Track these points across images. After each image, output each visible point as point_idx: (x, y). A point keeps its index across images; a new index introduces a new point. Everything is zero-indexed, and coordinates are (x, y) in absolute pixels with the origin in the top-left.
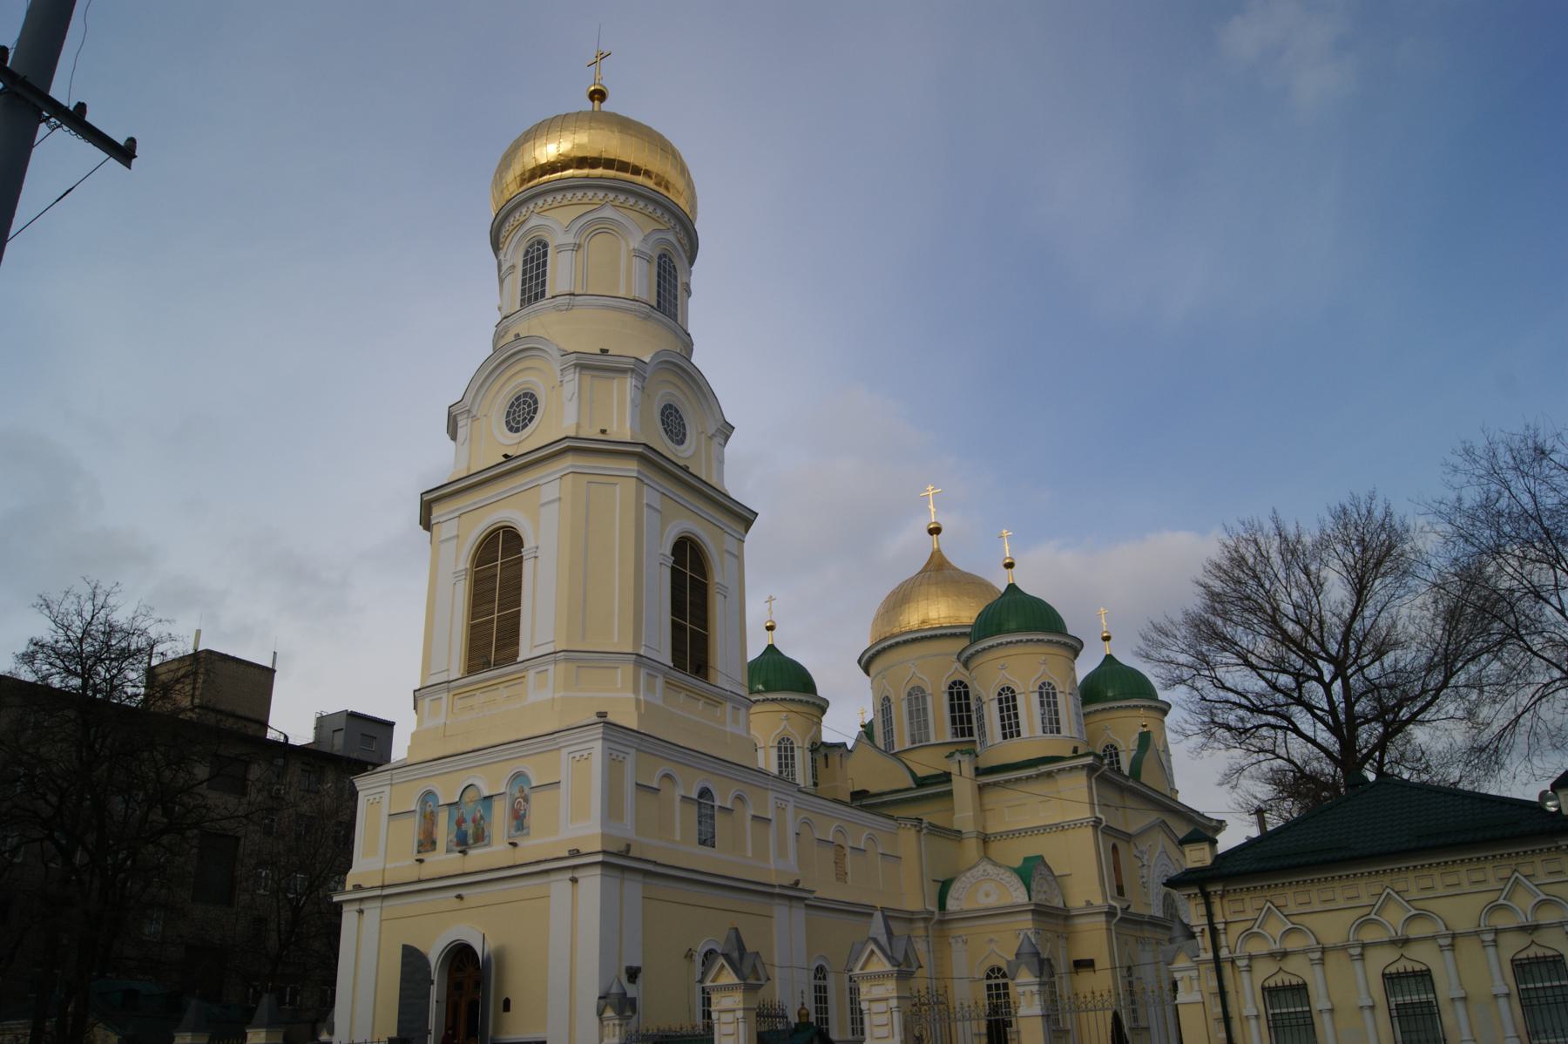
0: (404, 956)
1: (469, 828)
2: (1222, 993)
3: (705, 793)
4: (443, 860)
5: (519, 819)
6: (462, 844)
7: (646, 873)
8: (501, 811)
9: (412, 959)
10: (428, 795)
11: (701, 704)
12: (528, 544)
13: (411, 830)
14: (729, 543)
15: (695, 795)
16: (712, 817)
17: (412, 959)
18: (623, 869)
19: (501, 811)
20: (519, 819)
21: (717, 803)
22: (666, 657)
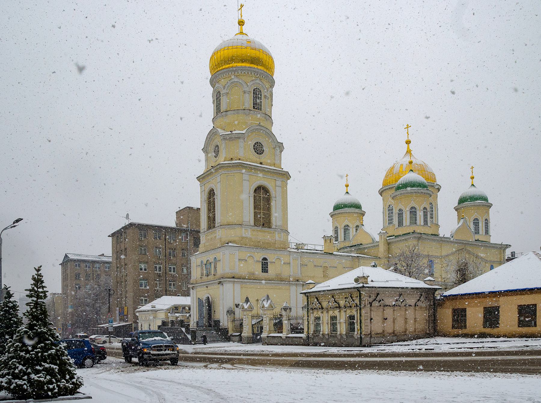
9: (200, 300)
14: (279, 183)
15: (261, 260)
17: (200, 300)
20: (215, 268)
21: (269, 260)
22: (252, 223)
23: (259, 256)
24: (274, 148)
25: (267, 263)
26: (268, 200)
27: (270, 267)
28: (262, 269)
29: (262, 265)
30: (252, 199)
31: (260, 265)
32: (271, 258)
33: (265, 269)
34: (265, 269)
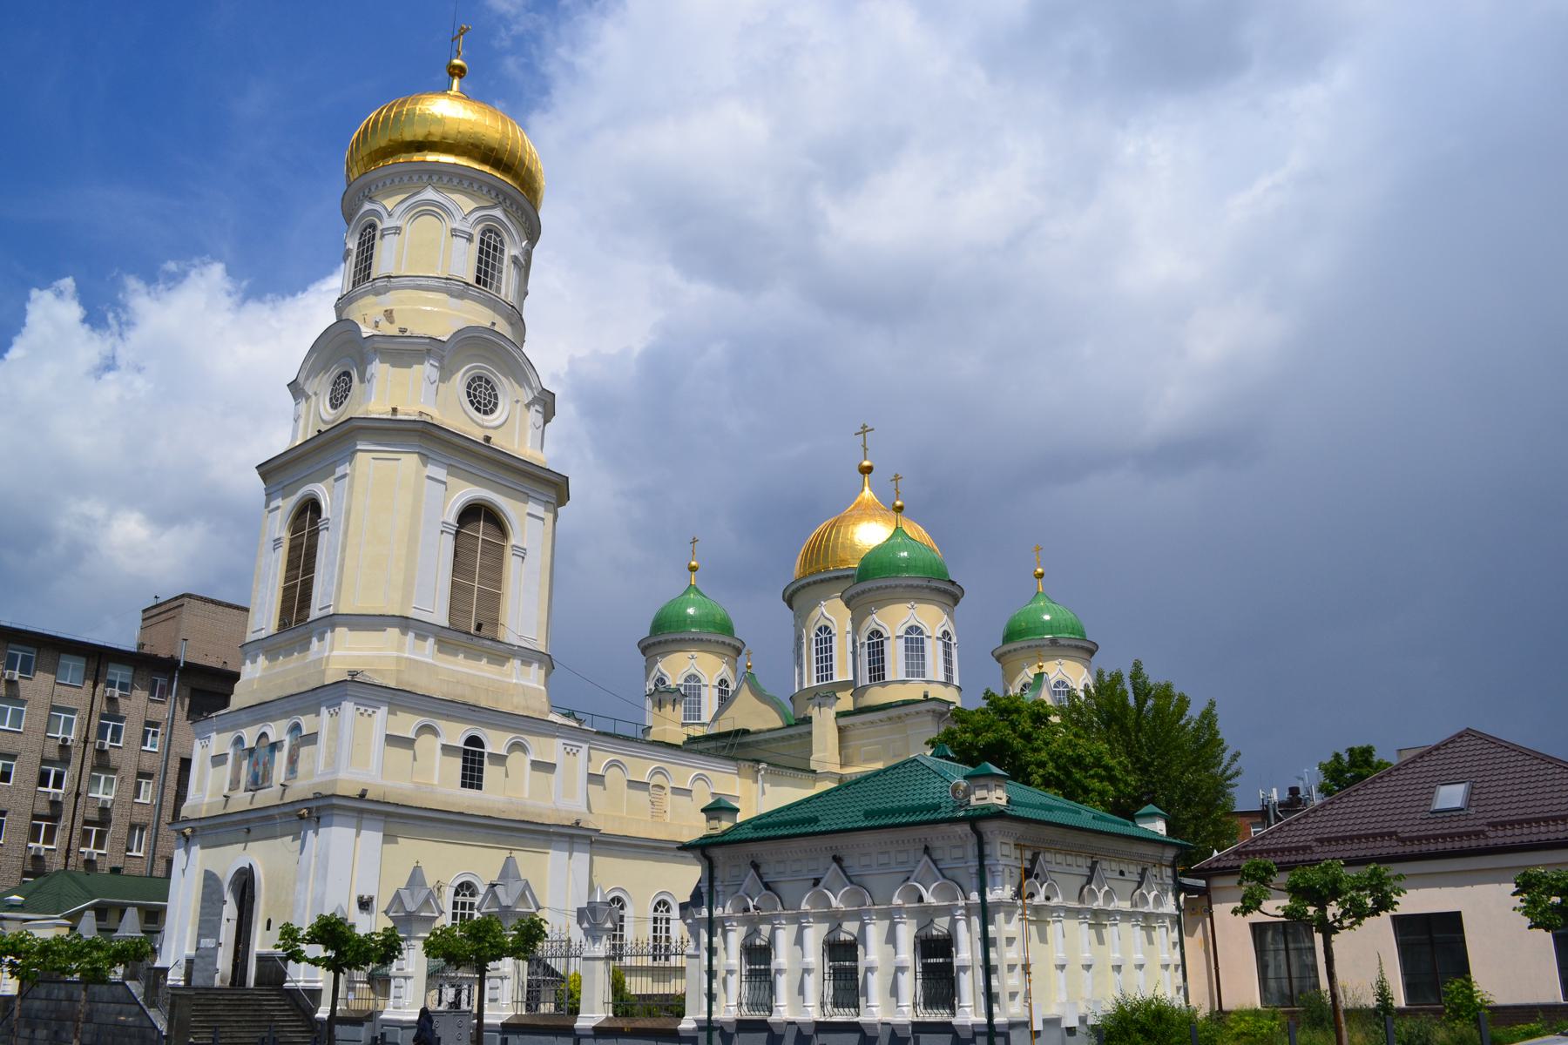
0: (205, 879)
1: (260, 769)
2: (712, 951)
3: (474, 741)
4: (242, 800)
5: (293, 761)
6: (257, 783)
7: (388, 815)
8: (282, 758)
10: (239, 741)
11: (485, 660)
12: (324, 516)
13: (227, 770)
15: (461, 745)
16: (481, 763)
17: (210, 879)
18: (361, 811)
19: (282, 758)
20: (293, 761)
21: (488, 749)
23: (456, 733)
24: (528, 406)
25: (482, 754)
26: (496, 556)
27: (490, 772)
28: (464, 776)
29: (465, 760)
30: (448, 543)
31: (457, 763)
32: (495, 741)
33: (472, 777)
34: (472, 777)
